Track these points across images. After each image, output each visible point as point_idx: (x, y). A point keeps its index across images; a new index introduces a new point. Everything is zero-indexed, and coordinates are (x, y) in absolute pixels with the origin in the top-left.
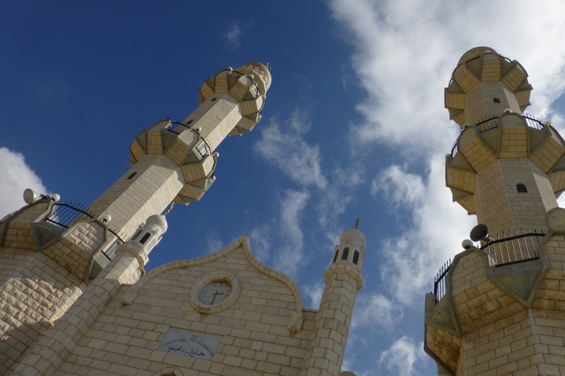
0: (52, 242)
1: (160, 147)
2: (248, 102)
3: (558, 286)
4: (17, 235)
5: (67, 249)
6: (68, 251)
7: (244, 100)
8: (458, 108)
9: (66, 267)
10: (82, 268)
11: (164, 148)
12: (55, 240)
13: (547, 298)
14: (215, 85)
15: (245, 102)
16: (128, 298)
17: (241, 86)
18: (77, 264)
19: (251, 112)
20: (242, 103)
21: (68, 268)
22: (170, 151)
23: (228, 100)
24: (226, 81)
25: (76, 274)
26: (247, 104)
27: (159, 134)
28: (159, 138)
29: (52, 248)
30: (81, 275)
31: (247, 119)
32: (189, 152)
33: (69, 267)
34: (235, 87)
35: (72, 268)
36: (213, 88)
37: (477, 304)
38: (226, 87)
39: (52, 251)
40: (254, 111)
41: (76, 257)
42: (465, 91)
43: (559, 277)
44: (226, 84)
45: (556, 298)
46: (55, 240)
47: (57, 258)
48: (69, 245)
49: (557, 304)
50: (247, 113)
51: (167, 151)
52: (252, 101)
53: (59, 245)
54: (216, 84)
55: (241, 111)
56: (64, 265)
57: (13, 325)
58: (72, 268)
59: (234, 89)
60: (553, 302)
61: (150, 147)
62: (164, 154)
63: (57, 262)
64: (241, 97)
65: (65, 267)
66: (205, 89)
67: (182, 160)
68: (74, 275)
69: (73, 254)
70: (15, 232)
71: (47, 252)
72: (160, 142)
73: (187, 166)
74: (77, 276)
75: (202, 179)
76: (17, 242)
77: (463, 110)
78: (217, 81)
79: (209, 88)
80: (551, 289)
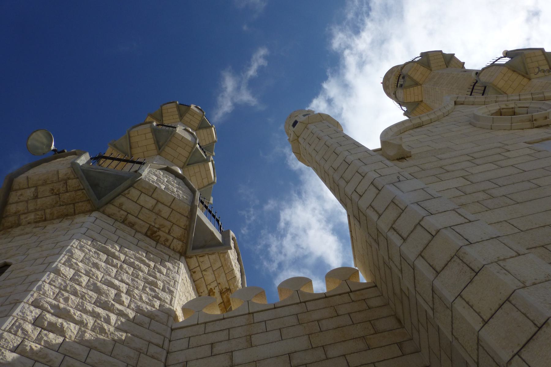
0: (121, 187)
1: (153, 147)
2: (205, 130)
4: (36, 197)
5: (148, 198)
8: (416, 100)
9: (149, 233)
10: (177, 232)
12: (128, 183)
15: (201, 131)
19: (208, 143)
21: (152, 234)
22: (168, 149)
24: (175, 109)
25: (168, 244)
27: (149, 130)
28: (150, 135)
29: (121, 199)
30: (178, 245)
32: (193, 148)
33: (156, 232)
34: (188, 115)
35: (160, 233)
38: (178, 116)
39: (120, 207)
41: (166, 212)
42: (421, 82)
44: (177, 113)
46: (128, 183)
47: (131, 218)
48: (152, 190)
52: (208, 130)
53: (134, 193)
54: (164, 115)
56: (144, 230)
57: (120, 314)
58: (160, 233)
59: (187, 118)
62: (159, 154)
63: (132, 225)
64: (196, 125)
65: (146, 234)
67: (184, 160)
68: (165, 245)
69: (160, 206)
70: (29, 193)
71: (111, 209)
72: (152, 141)
73: (191, 167)
74: (169, 247)
75: (209, 184)
76: (36, 210)
77: (422, 101)
78: (164, 111)
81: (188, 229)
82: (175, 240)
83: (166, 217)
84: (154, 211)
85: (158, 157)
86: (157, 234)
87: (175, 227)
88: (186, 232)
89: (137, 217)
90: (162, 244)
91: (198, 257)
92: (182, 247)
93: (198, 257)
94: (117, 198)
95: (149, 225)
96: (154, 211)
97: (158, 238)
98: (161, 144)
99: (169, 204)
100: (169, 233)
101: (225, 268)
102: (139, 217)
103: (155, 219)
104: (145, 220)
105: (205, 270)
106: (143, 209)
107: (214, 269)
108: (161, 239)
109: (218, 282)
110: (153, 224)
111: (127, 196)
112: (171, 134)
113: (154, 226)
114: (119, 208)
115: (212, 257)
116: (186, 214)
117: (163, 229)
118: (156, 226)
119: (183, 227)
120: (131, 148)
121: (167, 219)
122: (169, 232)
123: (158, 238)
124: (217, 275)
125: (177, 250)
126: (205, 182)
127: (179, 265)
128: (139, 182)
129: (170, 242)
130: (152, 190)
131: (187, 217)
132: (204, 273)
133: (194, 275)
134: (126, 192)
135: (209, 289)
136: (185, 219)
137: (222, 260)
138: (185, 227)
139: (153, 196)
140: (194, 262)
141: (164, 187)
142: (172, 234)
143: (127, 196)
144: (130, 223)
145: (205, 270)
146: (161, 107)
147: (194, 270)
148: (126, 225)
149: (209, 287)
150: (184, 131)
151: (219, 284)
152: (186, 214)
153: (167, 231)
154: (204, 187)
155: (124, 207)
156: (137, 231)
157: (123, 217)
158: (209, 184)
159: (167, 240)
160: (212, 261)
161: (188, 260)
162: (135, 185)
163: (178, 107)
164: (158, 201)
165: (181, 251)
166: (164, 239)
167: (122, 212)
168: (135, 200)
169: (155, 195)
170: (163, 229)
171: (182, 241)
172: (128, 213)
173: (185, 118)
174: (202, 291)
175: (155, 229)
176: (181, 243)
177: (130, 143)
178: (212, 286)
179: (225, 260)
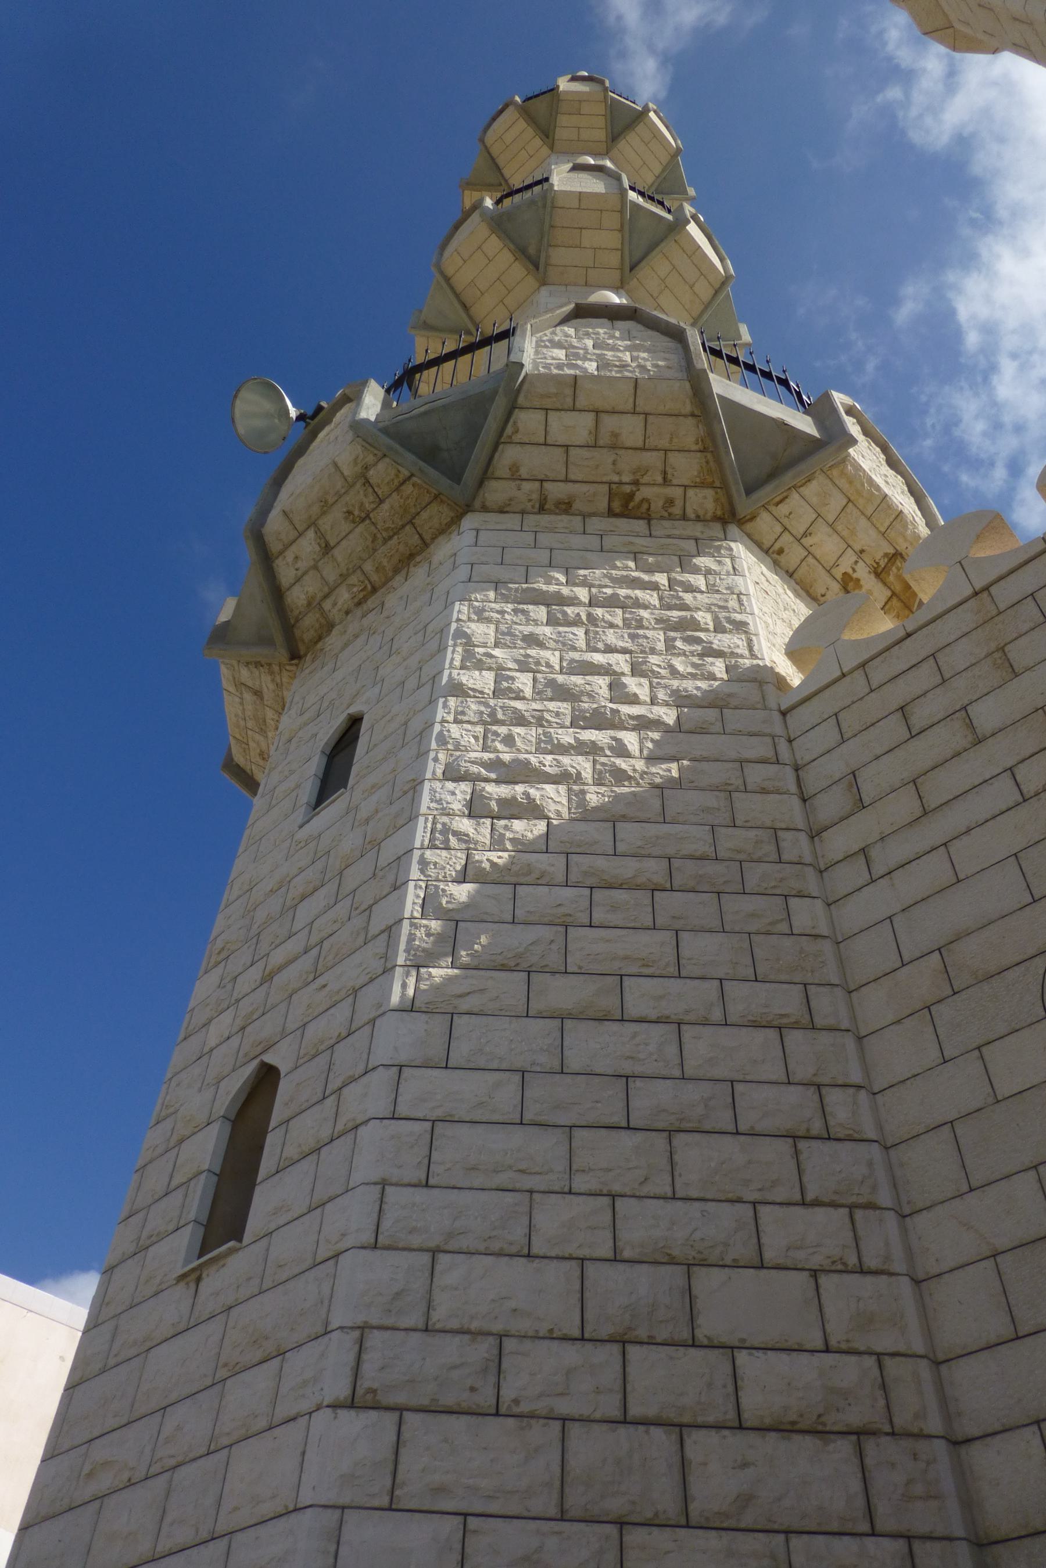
0: (492, 424)
1: (518, 270)
4: (327, 549)
5: (570, 418)
6: (579, 427)
9: (617, 506)
10: (686, 467)
15: (622, 144)
17: (579, 99)
18: (652, 459)
19: (658, 170)
21: (625, 505)
22: (559, 256)
24: (522, 124)
25: (677, 510)
27: (483, 230)
28: (494, 243)
29: (508, 455)
30: (703, 500)
32: (622, 211)
33: (631, 496)
34: (563, 120)
38: (538, 142)
39: (515, 475)
40: (665, 158)
41: (630, 429)
44: (530, 132)
47: (556, 491)
51: (547, 265)
52: (640, 128)
53: (528, 421)
56: (603, 504)
57: (642, 724)
58: (645, 492)
59: (566, 127)
62: (544, 283)
63: (565, 507)
64: (601, 135)
65: (611, 513)
67: (614, 259)
68: (671, 517)
69: (609, 423)
70: (308, 545)
71: (496, 491)
73: (644, 271)
74: (684, 517)
75: (717, 292)
76: (344, 577)
78: (495, 151)
81: (710, 446)
82: (691, 493)
83: (640, 444)
84: (601, 443)
85: (544, 291)
86: (638, 497)
87: (674, 459)
88: (709, 455)
89: (566, 480)
90: (662, 518)
91: (772, 508)
92: (716, 500)
93: (772, 508)
94: (497, 455)
95: (606, 487)
96: (601, 443)
97: (645, 506)
98: (532, 251)
99: (629, 406)
100: (666, 481)
101: (861, 502)
102: (572, 477)
103: (614, 463)
104: (591, 478)
105: (805, 535)
106: (573, 452)
107: (831, 518)
108: (653, 507)
109: (857, 548)
110: (616, 479)
111: (517, 438)
112: (544, 206)
113: (621, 483)
114: (512, 479)
115: (811, 490)
116: (688, 408)
117: (646, 479)
118: (626, 479)
119: (694, 447)
120: (465, 307)
121: (643, 449)
122: (665, 479)
123: (645, 506)
124: (845, 533)
125: (709, 516)
126: (704, 291)
127: (731, 549)
128: (525, 387)
129: (679, 503)
130: (569, 391)
131: (693, 415)
132: (807, 541)
133: (782, 559)
134: (509, 430)
135: (839, 576)
136: (690, 421)
137: (842, 483)
138: (700, 446)
139: (578, 405)
140: (765, 525)
141: (595, 364)
142: (675, 482)
143: (517, 438)
144: (558, 503)
145: (805, 535)
146: (482, 140)
147: (777, 546)
148: (550, 512)
149: (838, 573)
150: (572, 174)
151: (862, 551)
152: (688, 408)
153: (659, 479)
154: (707, 307)
155: (524, 472)
156: (585, 516)
157: (535, 496)
158: (717, 292)
159: (670, 502)
160: (814, 500)
161: (748, 526)
162: (521, 401)
163: (525, 111)
164: (597, 412)
165: (719, 513)
166: (660, 503)
167: (527, 486)
168: (542, 441)
169: (582, 402)
170: (646, 479)
171: (711, 486)
172: (542, 481)
173: (561, 134)
174: (821, 590)
175: (628, 489)
176: (709, 493)
177: (457, 296)
178: (845, 566)
179: (851, 483)
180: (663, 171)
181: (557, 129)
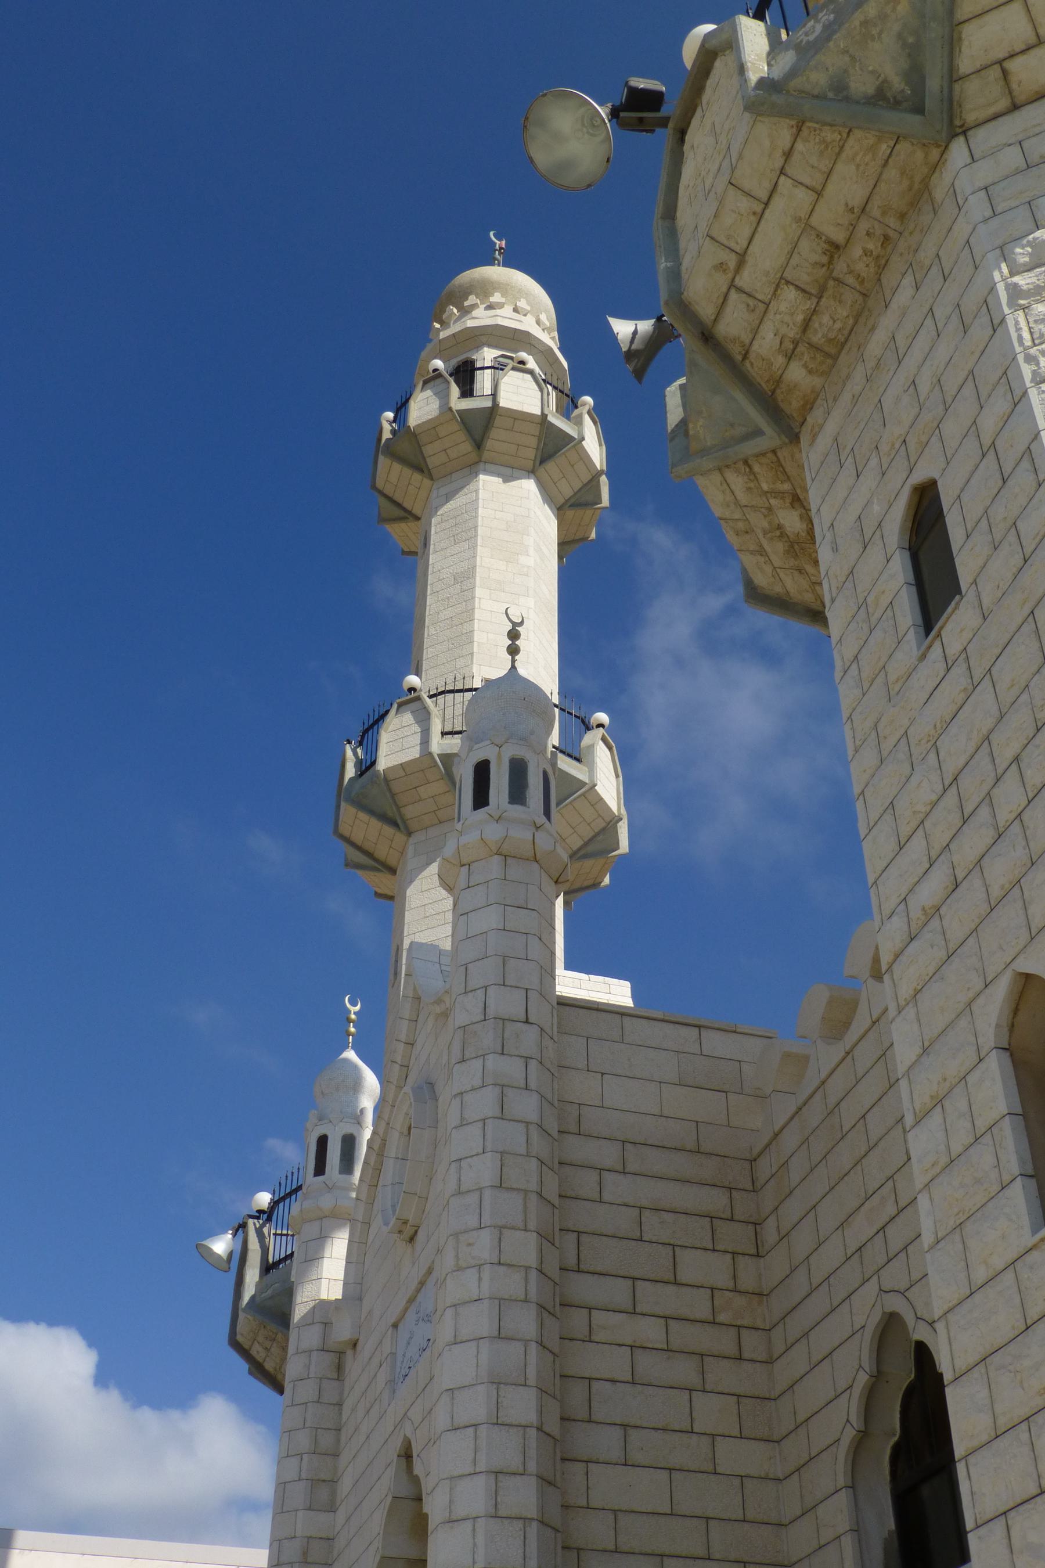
1: (388, 830)
2: (494, 433)
3: (751, 302)
7: (479, 445)
11: (394, 824)
13: (780, 360)
14: (399, 505)
15: (489, 444)
16: (343, 1332)
17: (432, 426)
19: (533, 442)
20: (486, 455)
22: (409, 812)
23: (448, 497)
26: (497, 441)
31: (551, 466)
34: (428, 450)
36: (409, 515)
37: (780, 546)
38: (417, 476)
43: (722, 281)
44: (407, 471)
45: (792, 333)
49: (817, 338)
50: (531, 454)
51: (404, 822)
52: (498, 421)
54: (398, 497)
55: (510, 471)
60: (801, 348)
61: (381, 853)
62: (409, 834)
64: (467, 447)
66: (399, 533)
79: (403, 525)
80: (755, 332)
146: (374, 486)
173: (432, 462)
180: (539, 441)
181: (428, 460)
